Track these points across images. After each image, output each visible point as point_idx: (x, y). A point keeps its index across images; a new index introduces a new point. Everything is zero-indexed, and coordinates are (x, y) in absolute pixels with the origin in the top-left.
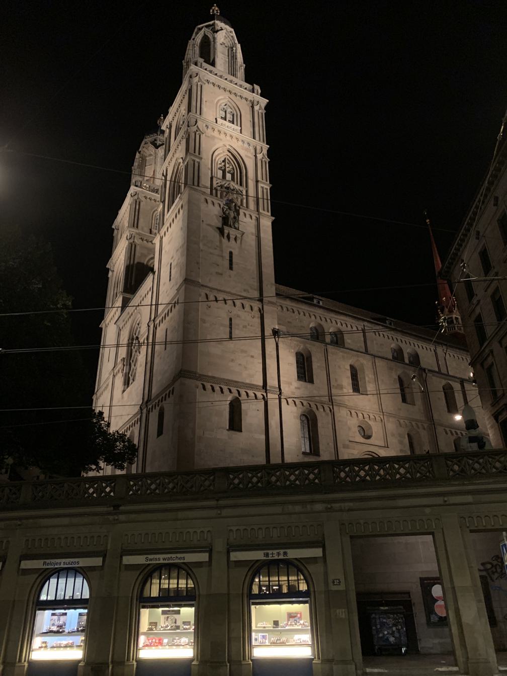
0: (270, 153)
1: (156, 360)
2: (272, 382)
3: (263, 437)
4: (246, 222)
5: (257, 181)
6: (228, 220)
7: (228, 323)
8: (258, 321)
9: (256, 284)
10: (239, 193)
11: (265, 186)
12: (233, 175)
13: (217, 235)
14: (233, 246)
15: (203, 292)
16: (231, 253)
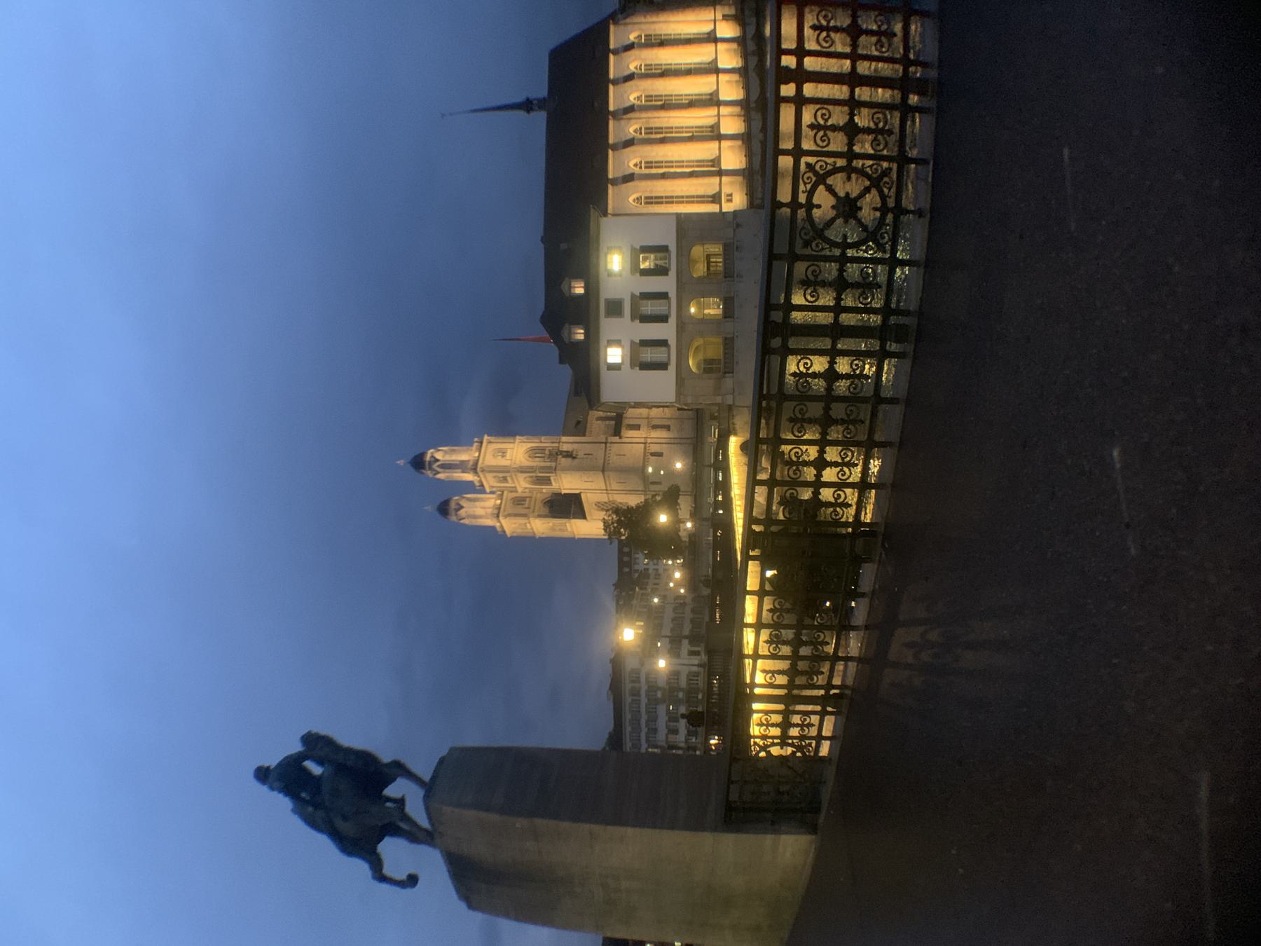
0: (521, 435)
1: (628, 489)
2: (643, 440)
3: (664, 445)
4: (565, 448)
5: (541, 442)
6: (569, 455)
7: (618, 457)
8: (616, 445)
9: (598, 445)
10: (550, 450)
11: (543, 439)
12: (536, 453)
13: (576, 461)
14: (581, 454)
15: (606, 464)
16: (585, 454)
